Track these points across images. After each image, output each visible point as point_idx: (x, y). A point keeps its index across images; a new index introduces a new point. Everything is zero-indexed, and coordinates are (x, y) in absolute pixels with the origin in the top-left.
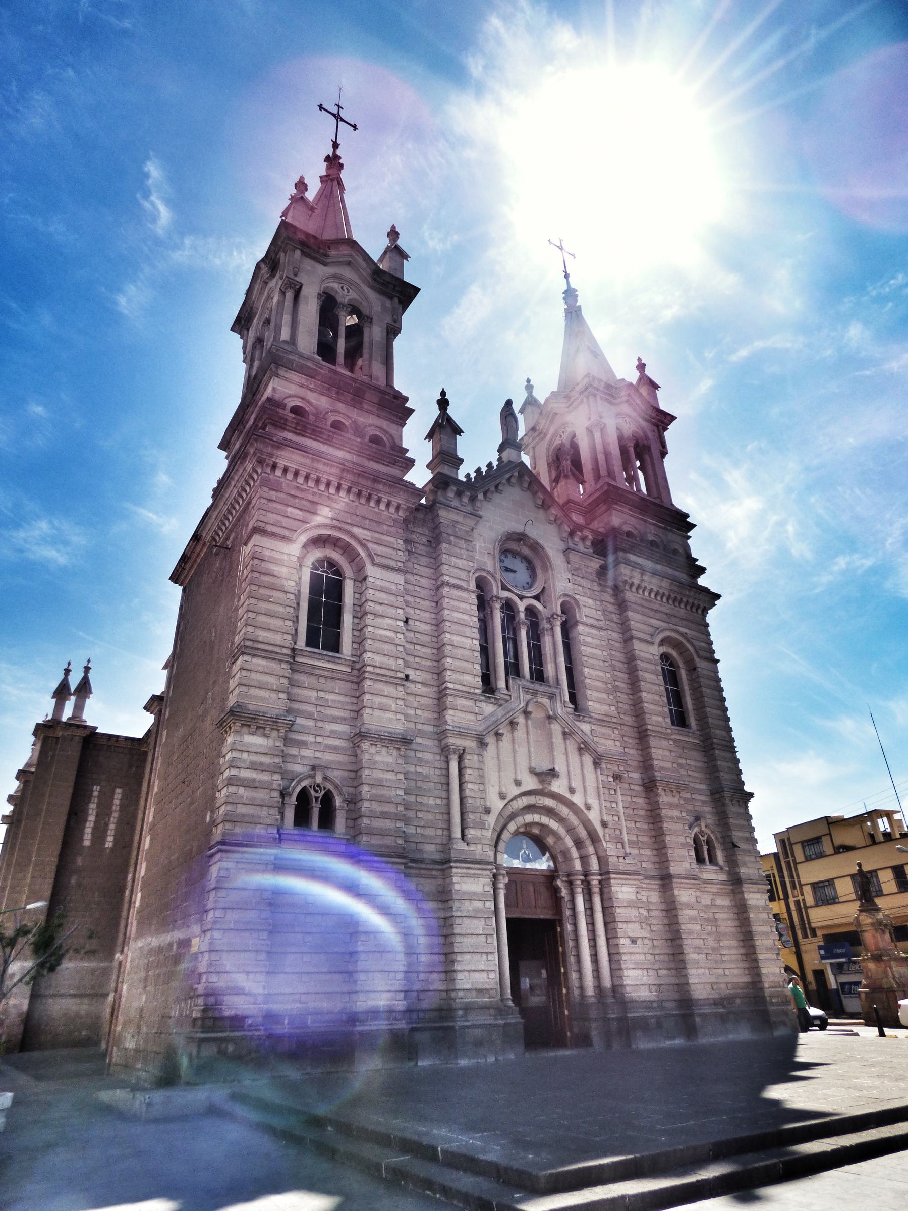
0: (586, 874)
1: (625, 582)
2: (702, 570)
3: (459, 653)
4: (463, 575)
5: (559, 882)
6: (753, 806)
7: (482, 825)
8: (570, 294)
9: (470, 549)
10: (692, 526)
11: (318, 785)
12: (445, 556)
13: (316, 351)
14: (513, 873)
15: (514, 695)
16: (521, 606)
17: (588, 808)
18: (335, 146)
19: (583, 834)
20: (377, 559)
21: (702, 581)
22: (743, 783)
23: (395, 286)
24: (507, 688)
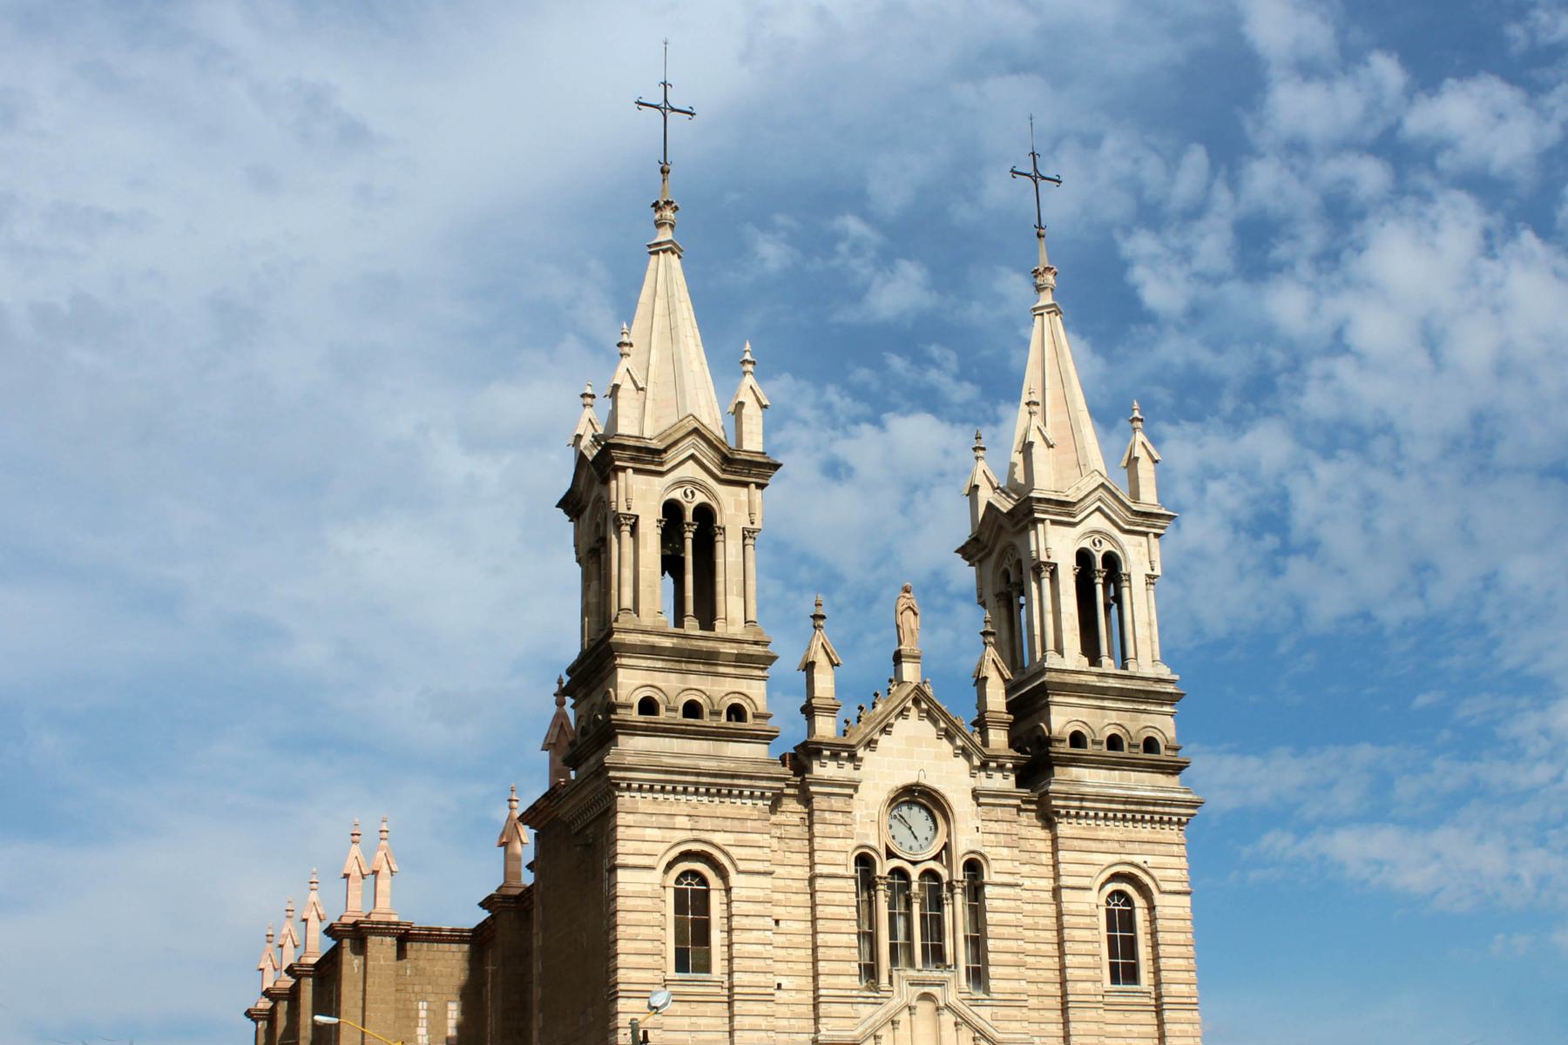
3: (833, 953)
4: (841, 858)
9: (848, 821)
15: (896, 989)
16: (915, 873)
24: (891, 982)
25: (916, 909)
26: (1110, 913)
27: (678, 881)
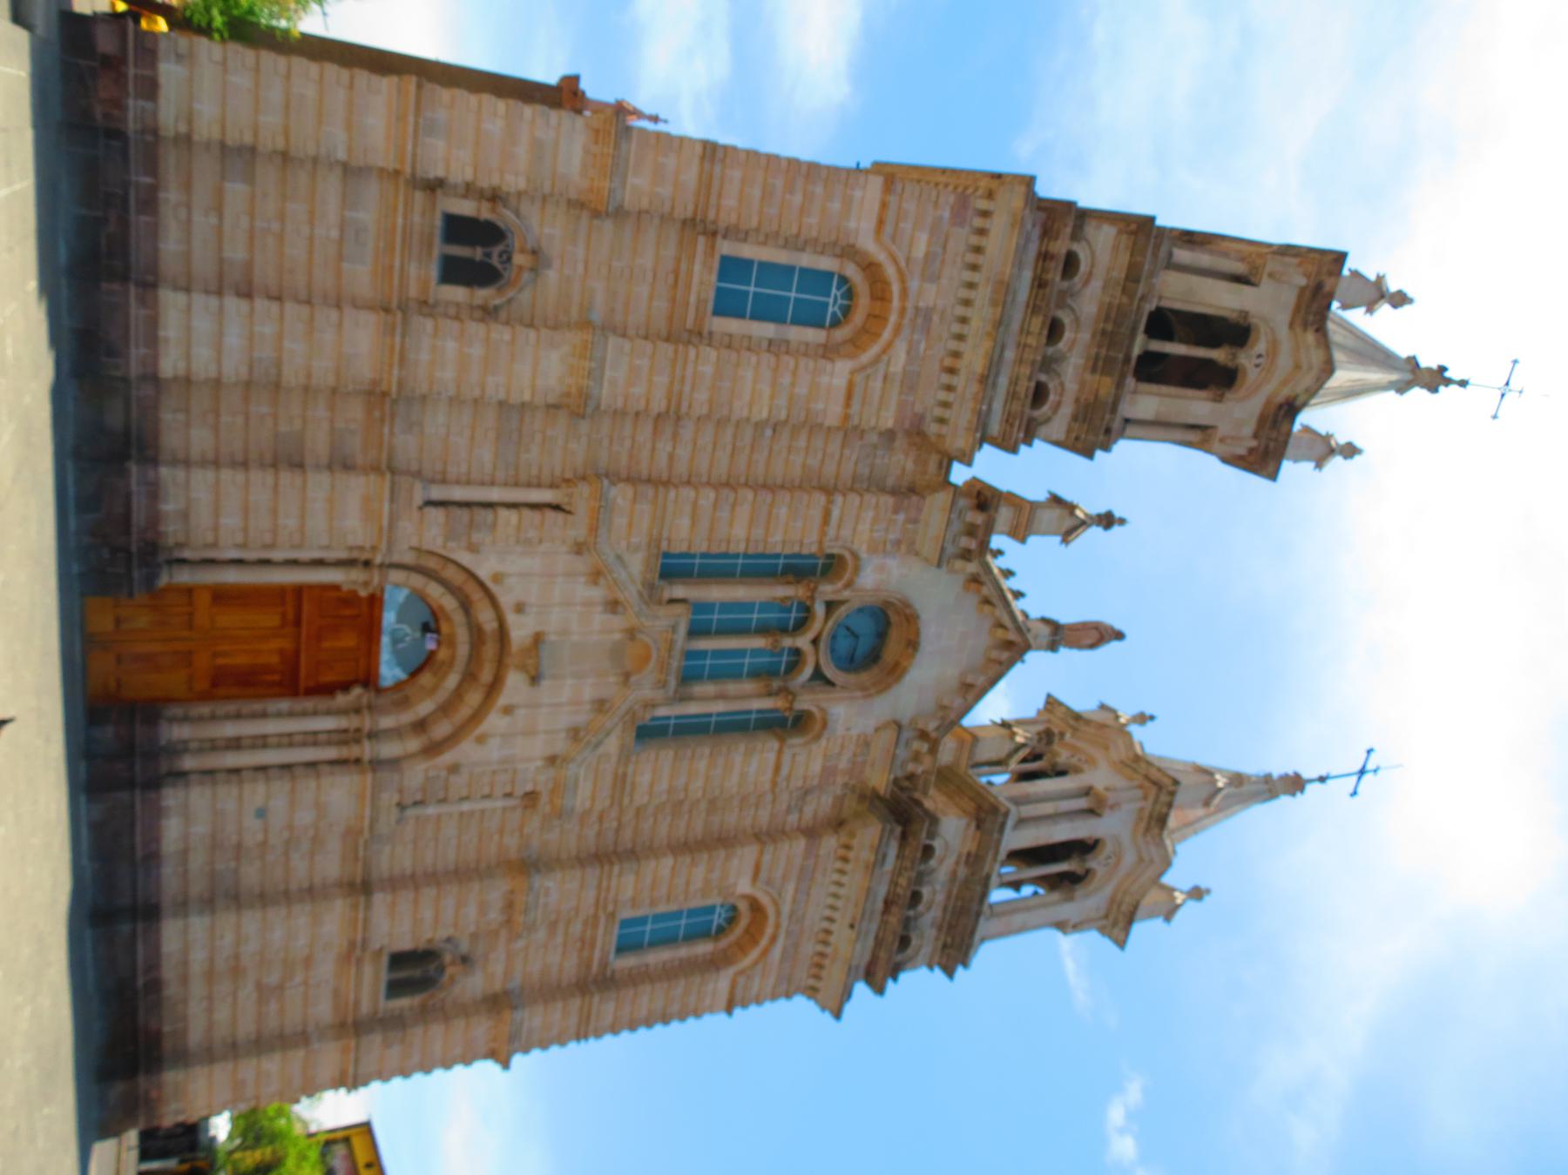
0: (373, 735)
1: (852, 835)
2: (880, 990)
5: (357, 691)
6: (486, 1069)
7: (450, 535)
8: (1295, 784)
10: (950, 972)
11: (509, 259)
12: (874, 500)
13: (1165, 304)
14: (375, 602)
15: (662, 611)
16: (803, 642)
17: (481, 740)
18: (1463, 383)
19: (442, 729)
20: (859, 378)
21: (861, 989)
22: (526, 1050)
23: (1276, 440)
24: (672, 601)
25: (759, 642)
26: (710, 910)
27: (844, 280)
